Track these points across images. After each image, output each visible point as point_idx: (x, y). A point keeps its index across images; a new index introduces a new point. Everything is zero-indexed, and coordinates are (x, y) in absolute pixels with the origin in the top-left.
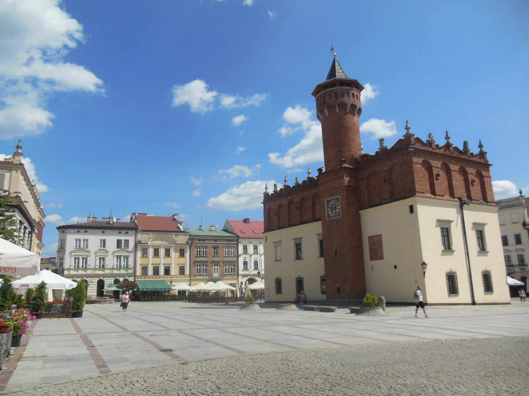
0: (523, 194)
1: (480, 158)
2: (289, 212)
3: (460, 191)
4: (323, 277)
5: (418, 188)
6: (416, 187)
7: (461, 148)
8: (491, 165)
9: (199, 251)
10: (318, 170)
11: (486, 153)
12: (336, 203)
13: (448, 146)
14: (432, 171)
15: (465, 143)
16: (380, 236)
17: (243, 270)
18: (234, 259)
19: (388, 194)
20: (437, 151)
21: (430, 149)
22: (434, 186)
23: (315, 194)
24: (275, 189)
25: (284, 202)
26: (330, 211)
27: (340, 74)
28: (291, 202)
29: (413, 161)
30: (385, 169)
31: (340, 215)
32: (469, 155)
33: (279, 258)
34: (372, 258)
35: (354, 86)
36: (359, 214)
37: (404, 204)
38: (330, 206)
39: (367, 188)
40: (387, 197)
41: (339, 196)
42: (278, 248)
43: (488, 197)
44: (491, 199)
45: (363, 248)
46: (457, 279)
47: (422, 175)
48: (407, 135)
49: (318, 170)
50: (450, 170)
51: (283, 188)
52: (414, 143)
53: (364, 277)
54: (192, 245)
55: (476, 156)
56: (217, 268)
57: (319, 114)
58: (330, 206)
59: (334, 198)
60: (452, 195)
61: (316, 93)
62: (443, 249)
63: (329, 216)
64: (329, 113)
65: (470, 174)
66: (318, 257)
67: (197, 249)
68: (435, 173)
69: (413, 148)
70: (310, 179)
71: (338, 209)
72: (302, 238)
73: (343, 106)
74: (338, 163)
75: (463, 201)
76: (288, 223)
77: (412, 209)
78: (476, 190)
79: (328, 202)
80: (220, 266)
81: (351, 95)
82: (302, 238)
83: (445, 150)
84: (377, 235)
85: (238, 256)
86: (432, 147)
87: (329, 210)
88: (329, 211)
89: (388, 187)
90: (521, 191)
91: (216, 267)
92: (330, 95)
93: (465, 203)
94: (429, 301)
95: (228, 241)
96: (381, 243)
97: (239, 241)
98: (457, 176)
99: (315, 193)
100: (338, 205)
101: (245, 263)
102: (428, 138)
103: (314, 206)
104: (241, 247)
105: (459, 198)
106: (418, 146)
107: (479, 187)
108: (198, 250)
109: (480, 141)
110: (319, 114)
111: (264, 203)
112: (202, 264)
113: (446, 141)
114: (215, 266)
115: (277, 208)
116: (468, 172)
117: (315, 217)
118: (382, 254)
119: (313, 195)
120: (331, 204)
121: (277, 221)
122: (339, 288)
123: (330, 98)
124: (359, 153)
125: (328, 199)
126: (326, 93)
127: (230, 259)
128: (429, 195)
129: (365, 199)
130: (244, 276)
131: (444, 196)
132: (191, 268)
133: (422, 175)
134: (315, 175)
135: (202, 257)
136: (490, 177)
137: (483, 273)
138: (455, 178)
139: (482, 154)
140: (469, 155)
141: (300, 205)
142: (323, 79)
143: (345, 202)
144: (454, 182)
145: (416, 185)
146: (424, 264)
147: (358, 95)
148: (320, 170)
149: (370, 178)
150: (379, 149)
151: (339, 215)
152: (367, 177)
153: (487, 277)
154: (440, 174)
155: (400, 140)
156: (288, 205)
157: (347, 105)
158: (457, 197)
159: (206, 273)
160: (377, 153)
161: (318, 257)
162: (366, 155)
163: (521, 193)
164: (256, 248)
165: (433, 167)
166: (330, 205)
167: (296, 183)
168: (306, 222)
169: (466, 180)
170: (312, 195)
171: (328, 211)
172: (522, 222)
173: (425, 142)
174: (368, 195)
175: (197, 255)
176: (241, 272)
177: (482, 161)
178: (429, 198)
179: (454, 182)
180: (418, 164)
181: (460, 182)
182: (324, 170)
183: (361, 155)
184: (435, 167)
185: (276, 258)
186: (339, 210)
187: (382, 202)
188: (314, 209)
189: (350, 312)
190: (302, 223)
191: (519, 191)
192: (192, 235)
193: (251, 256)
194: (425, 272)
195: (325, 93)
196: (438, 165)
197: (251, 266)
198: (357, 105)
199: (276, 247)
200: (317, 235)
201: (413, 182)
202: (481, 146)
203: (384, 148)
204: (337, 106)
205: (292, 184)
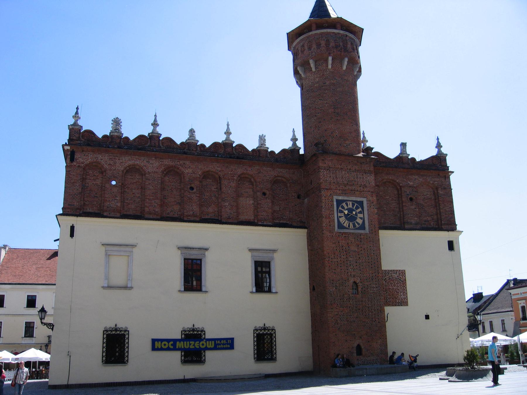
4: (261, 330)
26: (344, 218)
30: (411, 183)
40: (413, 221)
63: (340, 226)
72: (207, 249)
77: (451, 246)
82: (207, 249)
87: (339, 214)
96: (404, 282)
115: (123, 171)
120: (346, 207)
122: (359, 347)
125: (340, 198)
143: (376, 211)
151: (363, 227)
166: (343, 207)
200: (250, 250)
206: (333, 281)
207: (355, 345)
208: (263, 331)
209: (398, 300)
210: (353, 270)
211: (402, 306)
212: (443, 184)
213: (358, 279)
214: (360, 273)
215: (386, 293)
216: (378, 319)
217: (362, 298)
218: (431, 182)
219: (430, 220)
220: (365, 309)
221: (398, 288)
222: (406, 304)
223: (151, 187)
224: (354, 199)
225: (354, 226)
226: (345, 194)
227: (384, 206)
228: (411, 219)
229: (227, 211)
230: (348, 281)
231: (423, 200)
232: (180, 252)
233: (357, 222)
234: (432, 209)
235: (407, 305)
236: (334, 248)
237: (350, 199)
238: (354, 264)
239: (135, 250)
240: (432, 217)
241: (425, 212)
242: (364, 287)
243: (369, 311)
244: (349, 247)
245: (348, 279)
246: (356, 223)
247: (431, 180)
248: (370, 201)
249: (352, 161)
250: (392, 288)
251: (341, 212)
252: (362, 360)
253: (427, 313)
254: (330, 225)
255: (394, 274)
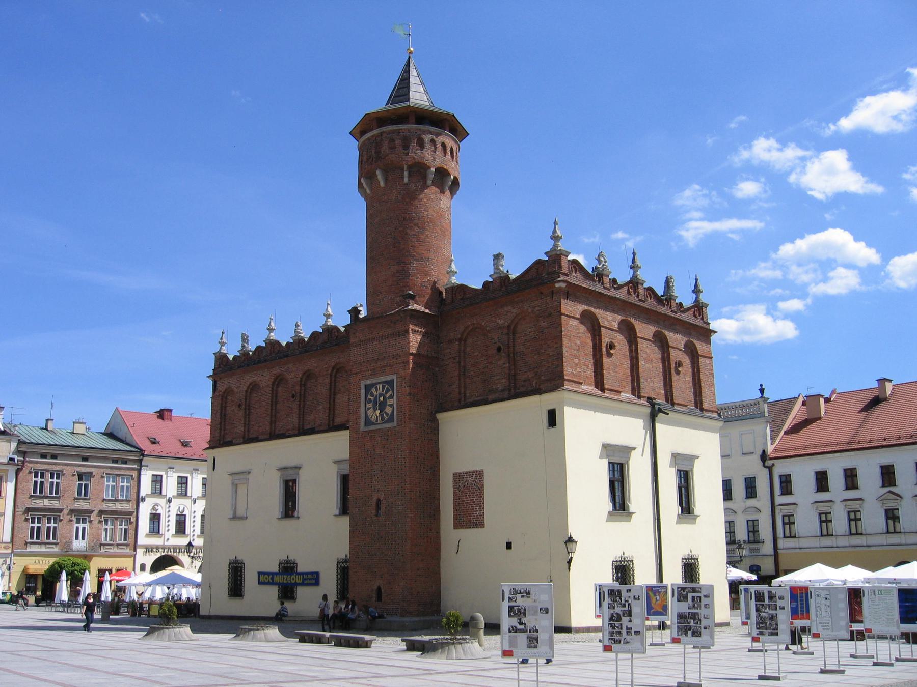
0: (765, 395)
1: (695, 316)
2: (274, 402)
3: (651, 385)
4: (343, 563)
5: (568, 371)
6: (565, 369)
7: (660, 291)
8: (715, 332)
9: (42, 483)
10: (349, 312)
11: (706, 306)
12: (386, 393)
13: (634, 284)
14: (600, 336)
15: (668, 282)
16: (480, 474)
17: (147, 536)
18: (128, 507)
19: (504, 381)
20: (613, 293)
21: (598, 288)
22: (602, 369)
23: (338, 367)
24: (243, 346)
25: (264, 378)
27: (417, 96)
28: (279, 380)
29: (563, 311)
30: (501, 322)
31: (393, 421)
32: (674, 308)
33: (241, 512)
34: (459, 523)
35: (448, 129)
36: (435, 421)
37: (537, 404)
38: (372, 398)
39: (459, 362)
40: (500, 387)
41: (394, 377)
42: (242, 490)
43: (704, 399)
44: (709, 404)
45: (439, 499)
46: (633, 574)
47: (578, 342)
48: (554, 253)
49: (349, 312)
50: (636, 337)
51: (264, 345)
52: (567, 272)
53: (439, 567)
54: (23, 466)
55: (688, 309)
56: (84, 529)
57: (362, 180)
58: (372, 398)
59: (383, 380)
60: (636, 390)
61: (359, 131)
62: (611, 509)
63: (368, 422)
64: (386, 180)
65: (673, 347)
66: (335, 516)
67: (36, 476)
68: (605, 340)
69: (564, 281)
70: (330, 331)
71: (391, 406)
72: (298, 468)
73: (419, 170)
74: (398, 299)
75: (657, 407)
76: (268, 429)
77: (552, 418)
78: (682, 384)
79: (368, 388)
80: (90, 522)
81: (439, 146)
82: (298, 468)
83: (629, 293)
84: (474, 472)
85: (139, 500)
86: (602, 284)
87: (368, 406)
88: (369, 409)
89: (504, 364)
90: (763, 387)
91: (81, 526)
92: (392, 140)
93: (660, 411)
94: (574, 624)
95: (115, 461)
96: (481, 489)
97: (143, 463)
98: (648, 352)
99: (337, 364)
100: (391, 397)
101: (155, 518)
102: (596, 264)
103: (335, 395)
104: (146, 478)
105: (650, 399)
106: (576, 279)
107: (689, 378)
108: (39, 480)
109: (696, 280)
110: (362, 180)
111: (216, 376)
112: (44, 516)
113: (632, 271)
114: (78, 522)
115: (246, 391)
116: (671, 344)
117: (333, 420)
118: (483, 515)
119: (333, 368)
120: (375, 394)
121: (242, 422)
122: (379, 589)
123: (392, 148)
124: (446, 281)
125: (368, 382)
126: (384, 135)
127: (118, 506)
128: (592, 389)
129: (454, 387)
130: (149, 549)
131: (620, 392)
132: (16, 525)
133: (578, 342)
134: (342, 321)
135: (47, 497)
136: (712, 358)
137: (685, 561)
138: (645, 356)
139: (699, 308)
140: (674, 308)
141: (300, 390)
142: (378, 103)
143: (408, 390)
144: (643, 363)
145: (565, 364)
146: (570, 540)
147: (455, 149)
148: (354, 312)
149: (465, 341)
150: (490, 276)
151: (391, 419)
152: (459, 336)
153: (692, 569)
154: (616, 344)
155: (539, 262)
156: (273, 385)
157: (429, 168)
158: (644, 397)
159: (54, 538)
160: (486, 284)
161: (335, 516)
162: (462, 288)
163: (762, 391)
164: (183, 482)
165: (603, 327)
166: (372, 395)
167: (296, 336)
168: (312, 431)
169: (666, 359)
170: (331, 368)
171: (366, 410)
172: (760, 452)
173: (590, 271)
174: (459, 380)
175: (35, 492)
176: (142, 540)
177: (698, 322)
178: (591, 395)
179: (642, 363)
180: (573, 317)
181: (654, 364)
182: (363, 314)
183: (451, 285)
184: (606, 328)
185: (235, 512)
186: (391, 409)
187: (490, 397)
188: (334, 400)
189: (405, 648)
190: (303, 431)
191: (760, 387)
192: (25, 443)
193: (170, 501)
194: (572, 558)
195: (381, 134)
196: (614, 323)
197: (168, 525)
198: (450, 170)
199: (235, 486)
200: (334, 462)
201: (560, 357)
202: (697, 290)
203: (502, 275)
204: (405, 167)
205: (284, 338)
206: (356, 499)
207: (375, 587)
208: (345, 564)
209: (473, 518)
210: (378, 482)
211: (477, 527)
212: (548, 308)
213: (382, 495)
214: (385, 486)
215: (460, 508)
216: (403, 551)
217: (385, 521)
218: (530, 310)
219: (532, 377)
220: (388, 537)
221: (473, 500)
222: (482, 525)
223: (264, 404)
224: (382, 379)
225: (383, 418)
226: (374, 374)
227: (472, 369)
228: (497, 384)
229: (319, 415)
230: (372, 499)
231: (523, 345)
232: (278, 474)
233: (385, 413)
234: (535, 357)
235: (484, 527)
236: (359, 454)
237: (379, 381)
238: (378, 473)
239: (250, 475)
240: (536, 370)
241: (526, 365)
242: (388, 506)
243: (392, 539)
244: (374, 450)
245: (372, 496)
246: (385, 415)
247: (529, 307)
248: (402, 377)
249: (385, 324)
250: (467, 501)
251: (370, 401)
252: (381, 608)
253: (509, 540)
254: (357, 423)
255: (470, 477)
